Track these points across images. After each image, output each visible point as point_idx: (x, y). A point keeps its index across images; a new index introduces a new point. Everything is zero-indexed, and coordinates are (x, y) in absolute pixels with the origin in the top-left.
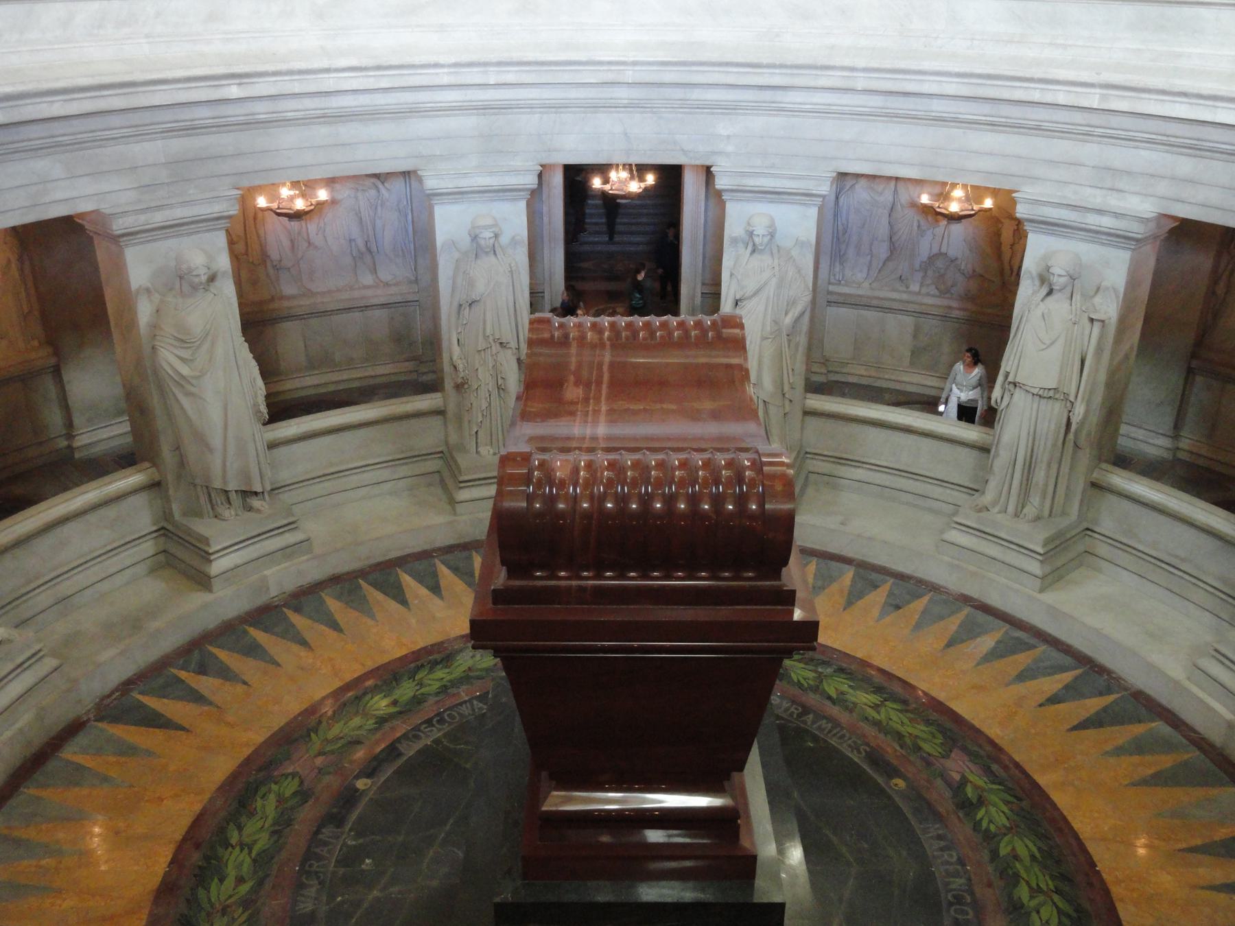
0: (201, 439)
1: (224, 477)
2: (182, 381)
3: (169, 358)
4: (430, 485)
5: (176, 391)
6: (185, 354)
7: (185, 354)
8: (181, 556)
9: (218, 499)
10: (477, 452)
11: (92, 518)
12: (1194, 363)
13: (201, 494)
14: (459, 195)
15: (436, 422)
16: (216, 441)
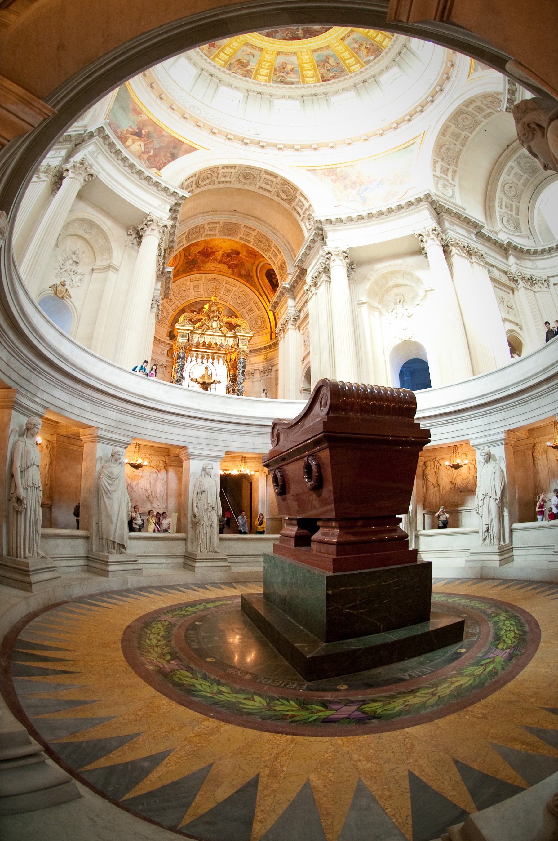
0: (109, 517)
1: (114, 536)
2: (108, 492)
3: (104, 481)
4: (180, 568)
5: (104, 495)
6: (110, 482)
7: (110, 482)
8: (95, 564)
9: (110, 544)
10: (201, 552)
11: (67, 541)
12: (424, 511)
13: (104, 542)
14: (199, 456)
15: (182, 543)
16: (114, 520)
